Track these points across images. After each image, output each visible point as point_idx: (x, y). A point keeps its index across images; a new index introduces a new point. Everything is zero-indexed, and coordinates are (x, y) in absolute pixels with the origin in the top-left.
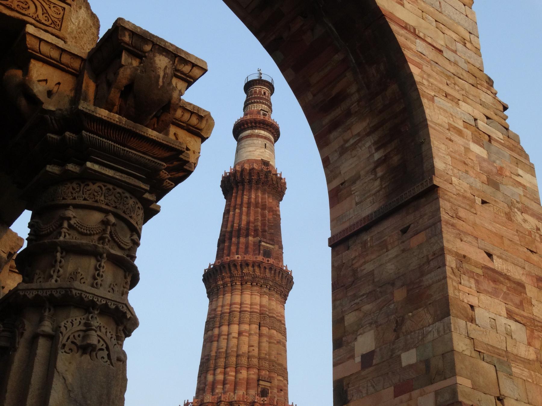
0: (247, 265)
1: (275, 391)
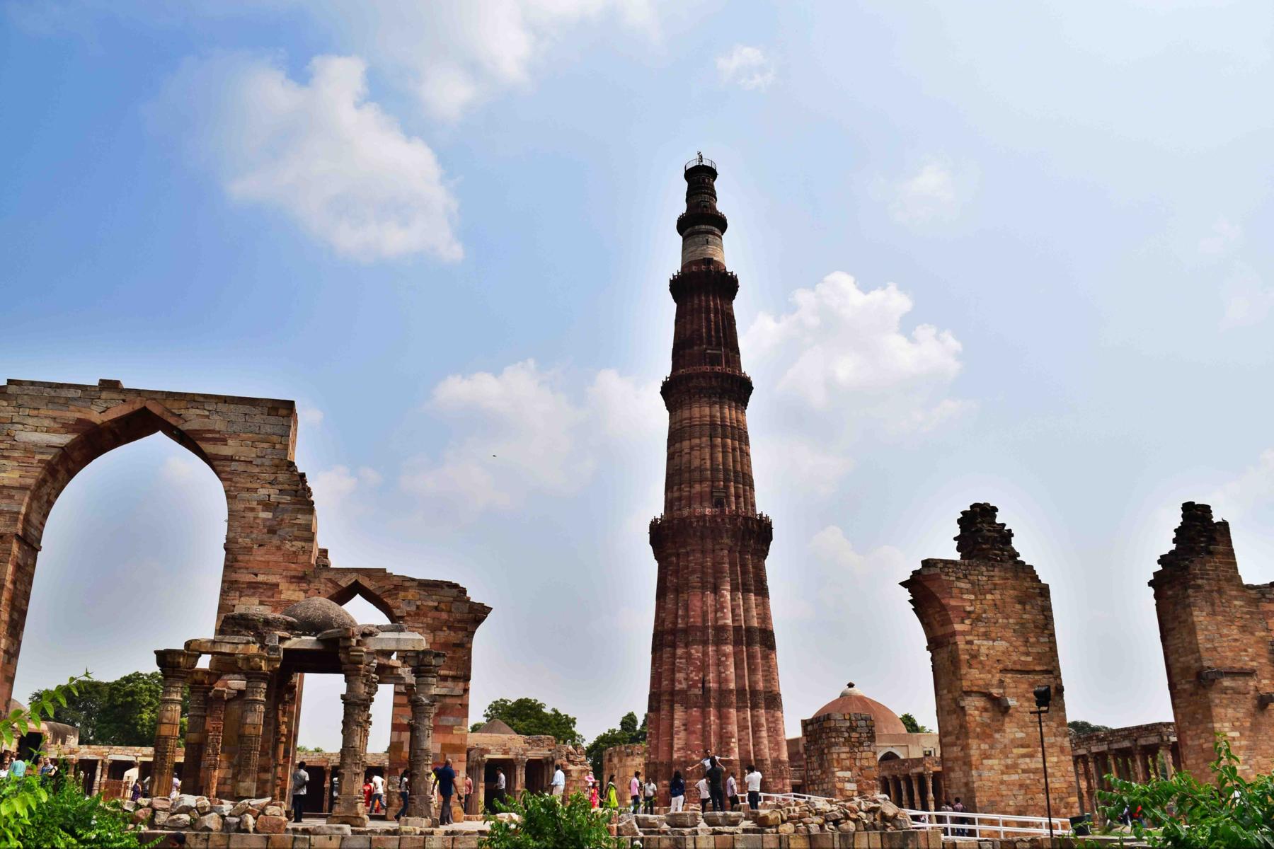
1: (733, 499)
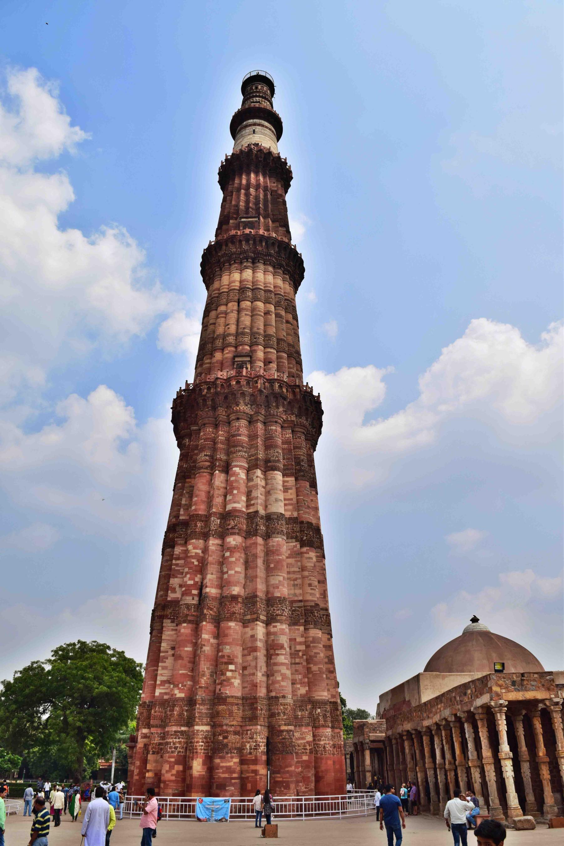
1: (261, 364)
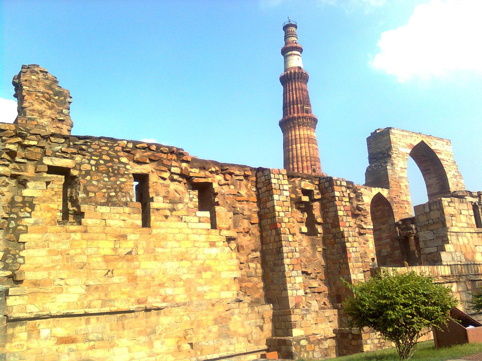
0: (300, 118)
1: (318, 169)
